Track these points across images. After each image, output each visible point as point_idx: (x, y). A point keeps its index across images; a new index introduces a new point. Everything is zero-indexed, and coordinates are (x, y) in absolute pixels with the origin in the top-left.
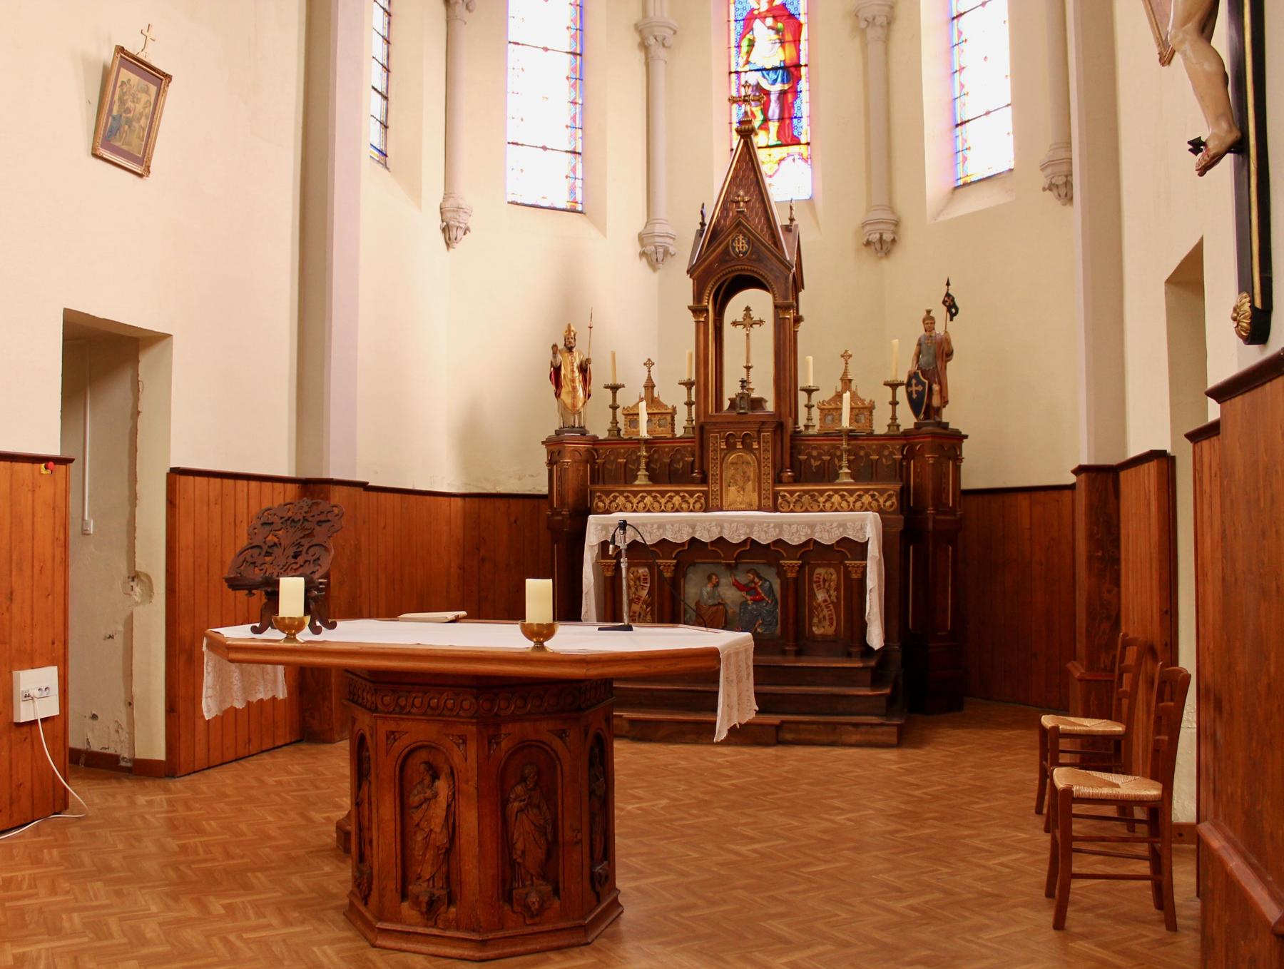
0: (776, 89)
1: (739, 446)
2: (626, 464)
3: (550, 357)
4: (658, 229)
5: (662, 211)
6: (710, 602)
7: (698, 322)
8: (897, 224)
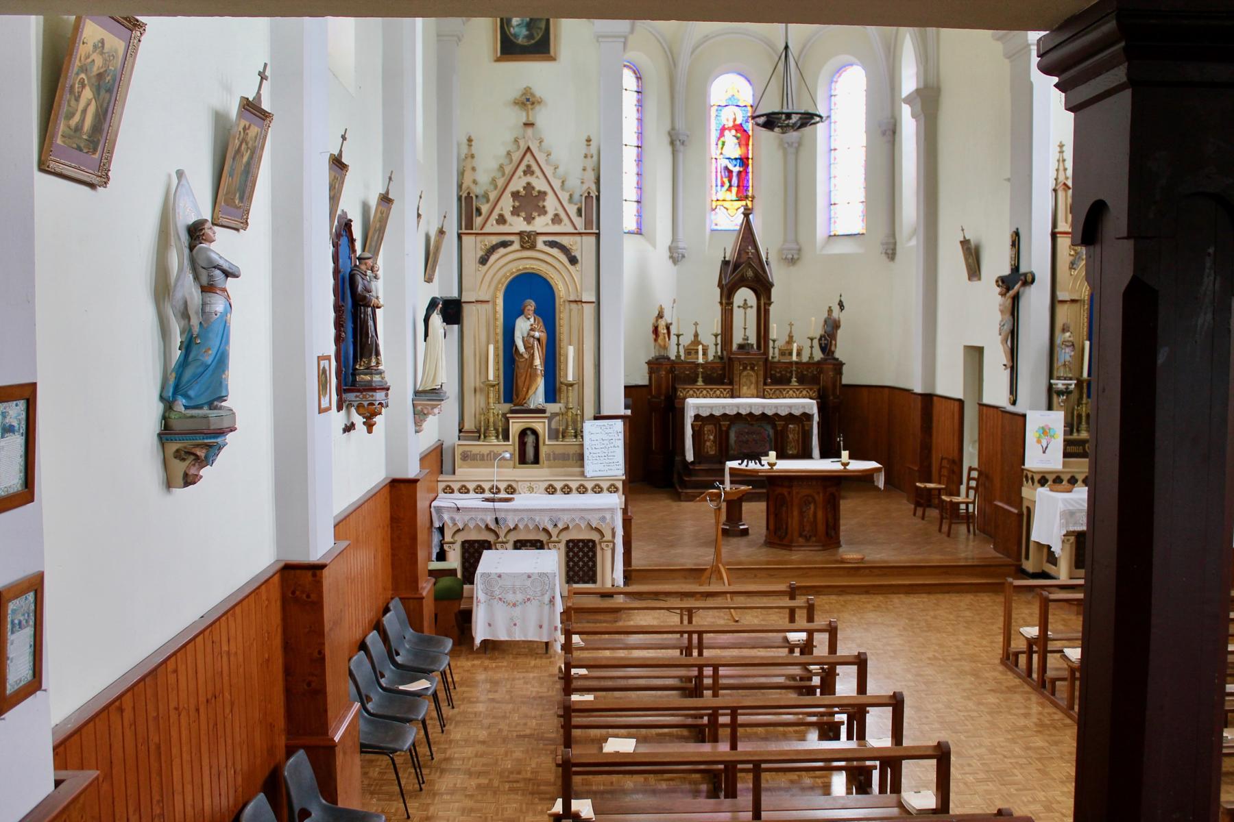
0: (736, 169)
5: (681, 235)
8: (800, 250)
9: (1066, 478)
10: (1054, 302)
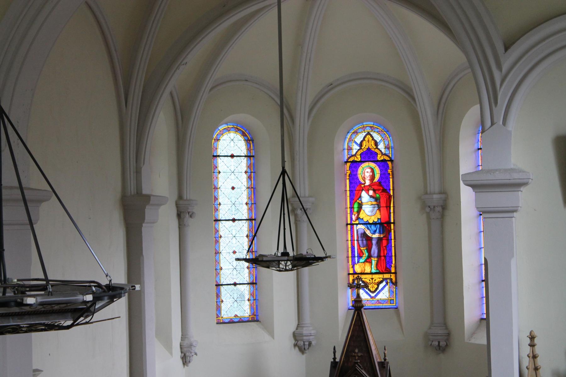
5: (307, 319)
8: (449, 335)
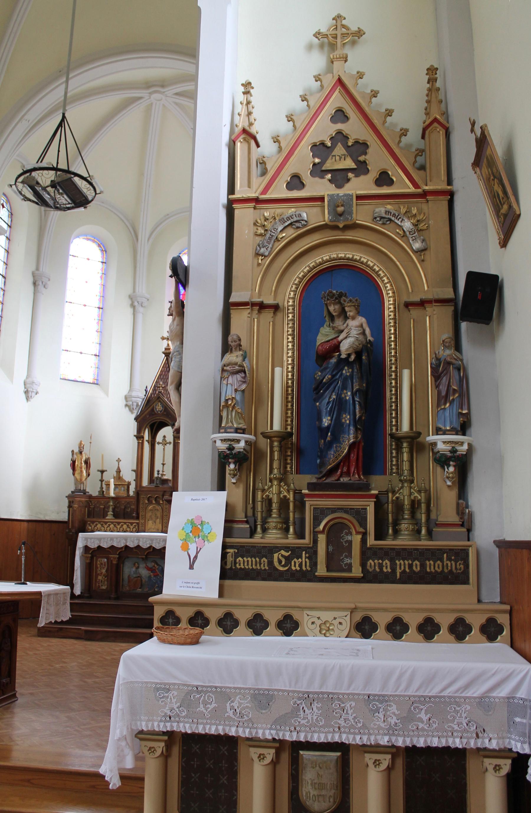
1: (154, 502)
2: (104, 508)
3: (71, 457)
4: (134, 394)
6: (135, 576)
7: (138, 443)
9: (214, 615)
10: (229, 307)
